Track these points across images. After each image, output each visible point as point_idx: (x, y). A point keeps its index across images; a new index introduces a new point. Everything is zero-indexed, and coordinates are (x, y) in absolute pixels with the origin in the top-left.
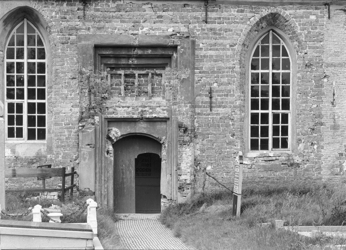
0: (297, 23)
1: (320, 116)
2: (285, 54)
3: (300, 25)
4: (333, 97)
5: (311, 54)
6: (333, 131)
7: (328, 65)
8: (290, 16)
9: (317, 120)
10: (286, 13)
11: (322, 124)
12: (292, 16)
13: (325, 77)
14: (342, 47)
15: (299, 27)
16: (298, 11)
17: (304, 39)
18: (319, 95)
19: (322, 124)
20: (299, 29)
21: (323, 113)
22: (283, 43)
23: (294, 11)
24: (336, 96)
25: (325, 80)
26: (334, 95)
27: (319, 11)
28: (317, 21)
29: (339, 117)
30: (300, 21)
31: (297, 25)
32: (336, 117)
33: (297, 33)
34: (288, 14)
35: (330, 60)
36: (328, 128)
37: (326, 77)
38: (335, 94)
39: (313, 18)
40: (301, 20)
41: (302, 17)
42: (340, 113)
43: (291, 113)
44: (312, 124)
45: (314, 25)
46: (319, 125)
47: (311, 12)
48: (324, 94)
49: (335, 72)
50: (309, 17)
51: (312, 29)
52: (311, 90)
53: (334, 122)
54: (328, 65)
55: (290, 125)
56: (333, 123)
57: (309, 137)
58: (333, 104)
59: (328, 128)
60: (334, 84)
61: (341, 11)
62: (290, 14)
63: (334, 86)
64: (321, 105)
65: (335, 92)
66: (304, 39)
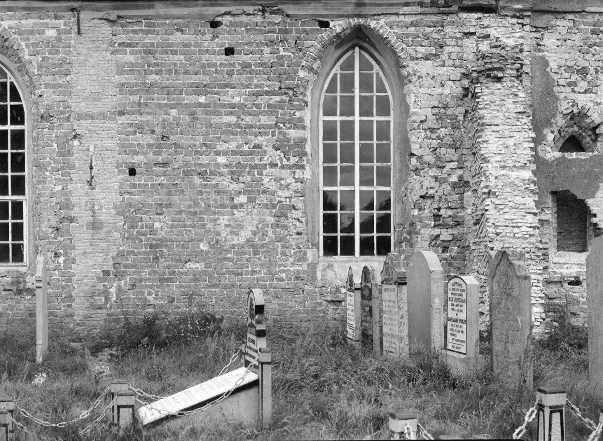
0: (23, 44)
1: (68, 206)
2: (15, 96)
3: (28, 46)
4: (91, 173)
5: (50, 97)
6: (93, 231)
7: (80, 117)
8: (9, 30)
9: (63, 213)
10: (3, 26)
11: (71, 220)
12: (13, 31)
13: (75, 137)
14: (106, 84)
15: (27, 50)
16: (23, 21)
17: (36, 71)
18: (66, 169)
19: (71, 220)
20: (27, 53)
21: (74, 200)
22: (12, 77)
23: (17, 22)
24: (94, 171)
25: (76, 143)
26: (91, 168)
27: (62, 21)
28: (58, 39)
29: (102, 207)
30: (28, 39)
31: (24, 47)
32: (96, 207)
33: (23, 60)
34: (7, 28)
35: (83, 107)
36: (83, 226)
37: (77, 137)
38: (94, 167)
39: (51, 33)
40: (31, 37)
41: (31, 32)
42: (103, 201)
43: (26, 200)
44: (54, 221)
45: (53, 46)
46: (66, 220)
47: (47, 24)
48: (73, 167)
49: (93, 129)
50: (43, 33)
51: (50, 53)
52: (52, 161)
53: (92, 216)
54: (80, 117)
55: (25, 221)
56: (91, 219)
57: (50, 243)
58: (91, 185)
59: (83, 226)
60: (92, 148)
61: (103, 21)
62: (10, 28)
63: (91, 154)
64: (69, 187)
65: (94, 164)
66: (36, 71)
